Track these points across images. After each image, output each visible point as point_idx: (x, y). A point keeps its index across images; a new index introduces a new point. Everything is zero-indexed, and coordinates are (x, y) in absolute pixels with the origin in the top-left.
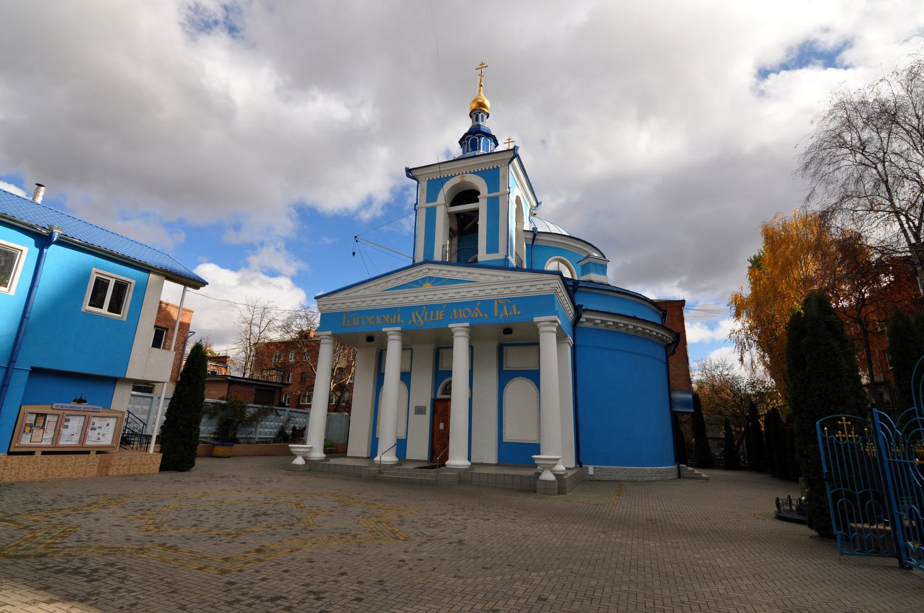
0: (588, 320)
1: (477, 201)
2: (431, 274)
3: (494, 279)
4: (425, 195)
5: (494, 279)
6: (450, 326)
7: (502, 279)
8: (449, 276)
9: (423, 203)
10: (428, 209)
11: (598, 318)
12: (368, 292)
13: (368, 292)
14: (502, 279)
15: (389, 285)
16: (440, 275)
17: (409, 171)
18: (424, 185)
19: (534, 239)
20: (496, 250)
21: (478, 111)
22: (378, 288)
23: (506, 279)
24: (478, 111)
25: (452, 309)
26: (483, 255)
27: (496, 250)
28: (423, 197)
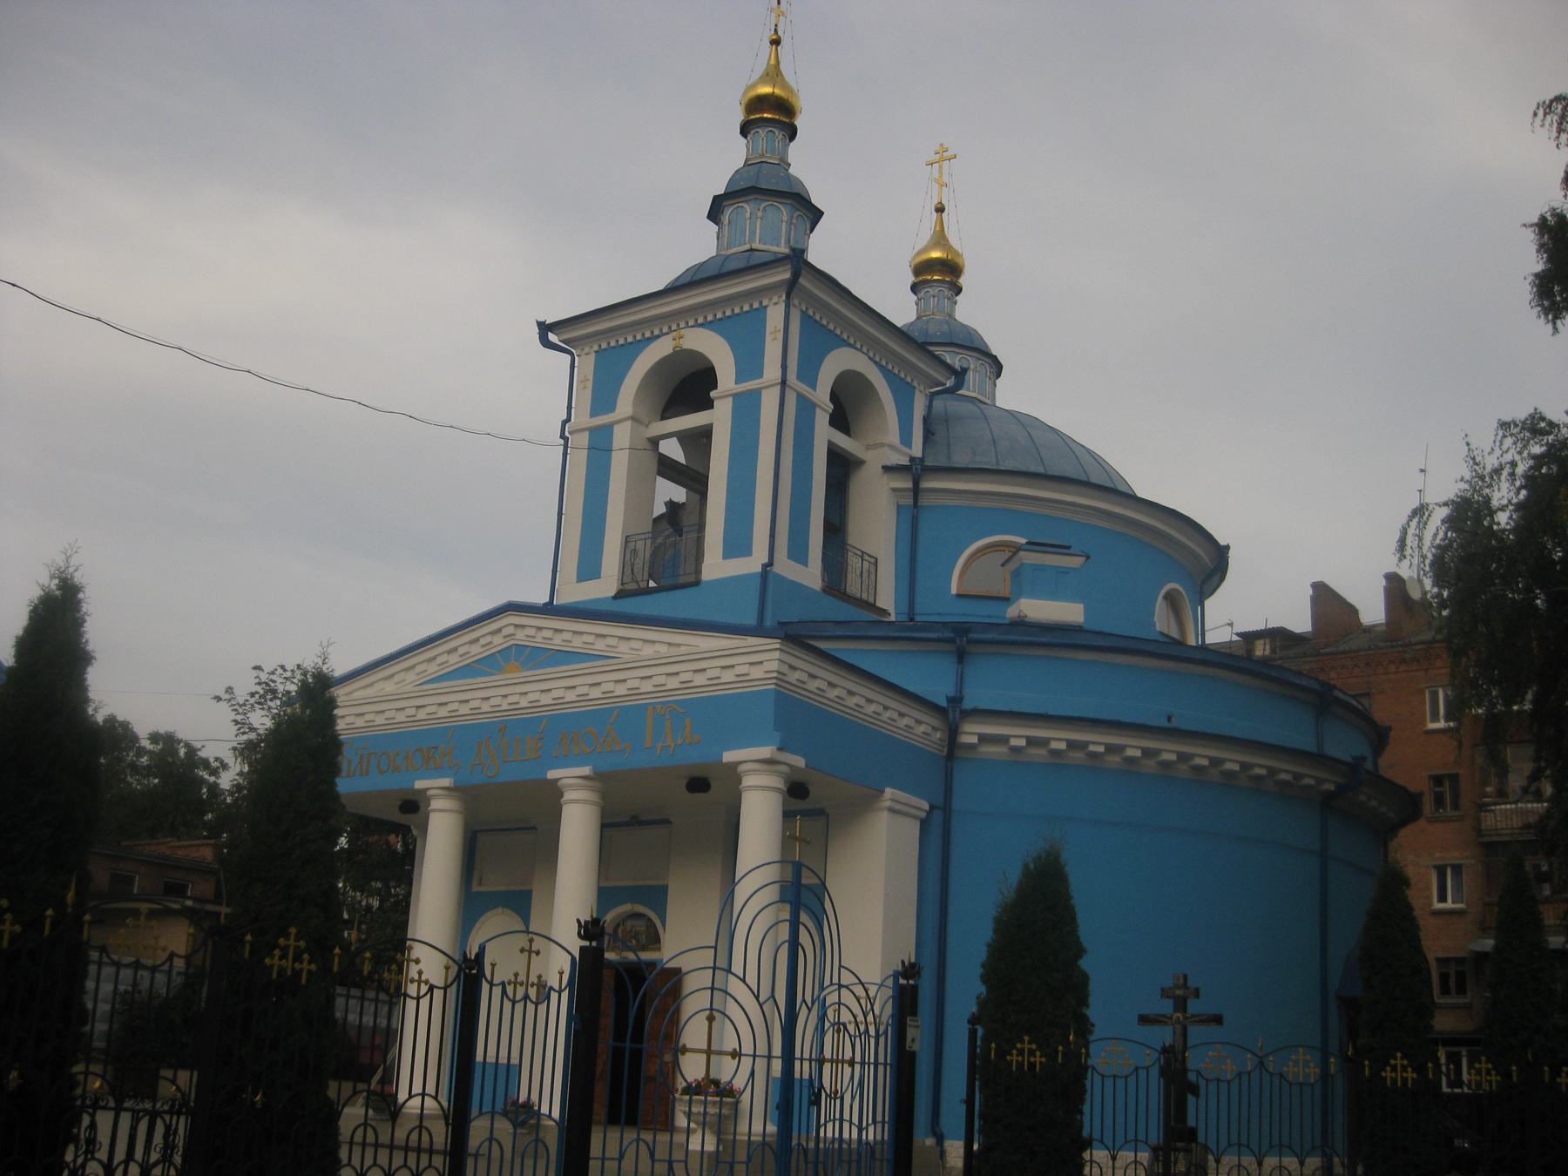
0: (984, 739)
1: (708, 404)
2: (521, 637)
3: (648, 651)
4: (588, 394)
5: (648, 651)
6: (552, 774)
7: (664, 649)
8: (558, 642)
9: (582, 417)
10: (593, 431)
11: (1018, 734)
12: (389, 687)
13: (389, 687)
14: (664, 649)
15: (432, 668)
16: (539, 640)
17: (544, 328)
18: (587, 364)
19: (916, 490)
20: (747, 552)
21: (771, 115)
22: (411, 677)
23: (674, 651)
24: (771, 115)
25: (566, 731)
26: (715, 566)
27: (747, 552)
28: (583, 399)
